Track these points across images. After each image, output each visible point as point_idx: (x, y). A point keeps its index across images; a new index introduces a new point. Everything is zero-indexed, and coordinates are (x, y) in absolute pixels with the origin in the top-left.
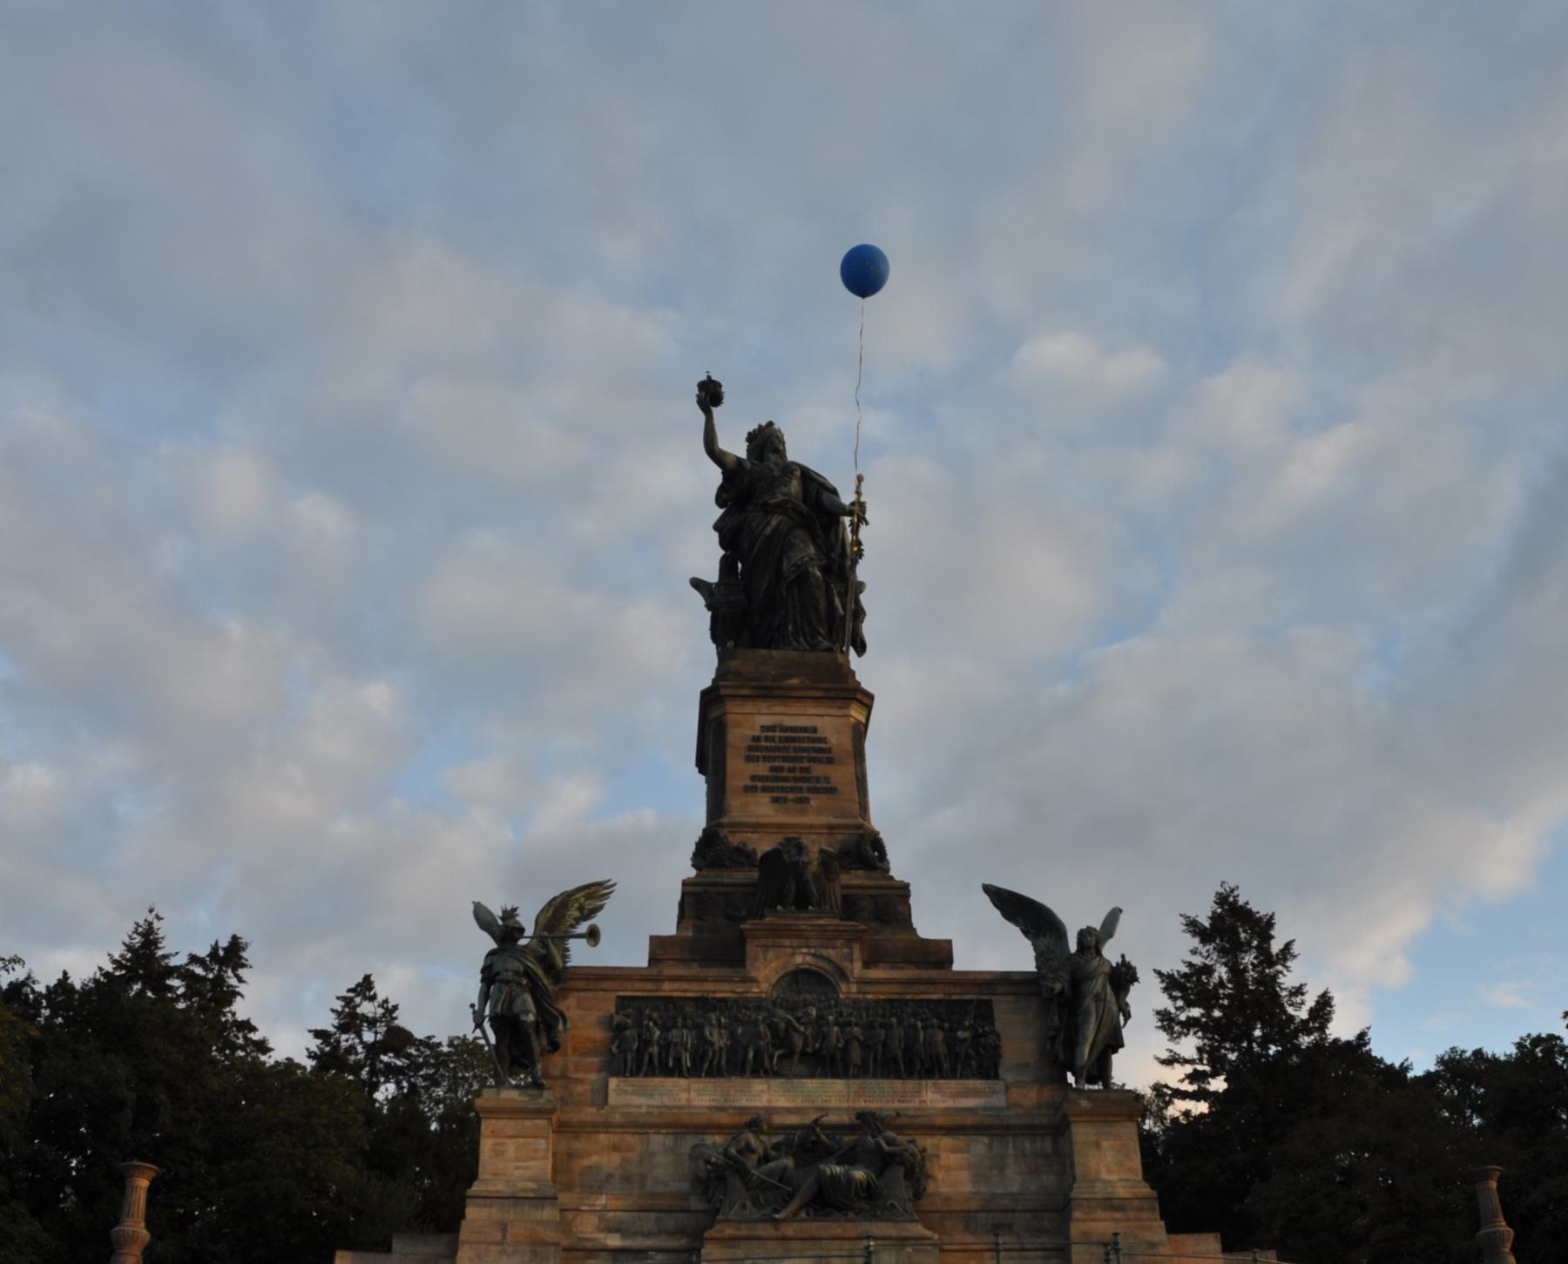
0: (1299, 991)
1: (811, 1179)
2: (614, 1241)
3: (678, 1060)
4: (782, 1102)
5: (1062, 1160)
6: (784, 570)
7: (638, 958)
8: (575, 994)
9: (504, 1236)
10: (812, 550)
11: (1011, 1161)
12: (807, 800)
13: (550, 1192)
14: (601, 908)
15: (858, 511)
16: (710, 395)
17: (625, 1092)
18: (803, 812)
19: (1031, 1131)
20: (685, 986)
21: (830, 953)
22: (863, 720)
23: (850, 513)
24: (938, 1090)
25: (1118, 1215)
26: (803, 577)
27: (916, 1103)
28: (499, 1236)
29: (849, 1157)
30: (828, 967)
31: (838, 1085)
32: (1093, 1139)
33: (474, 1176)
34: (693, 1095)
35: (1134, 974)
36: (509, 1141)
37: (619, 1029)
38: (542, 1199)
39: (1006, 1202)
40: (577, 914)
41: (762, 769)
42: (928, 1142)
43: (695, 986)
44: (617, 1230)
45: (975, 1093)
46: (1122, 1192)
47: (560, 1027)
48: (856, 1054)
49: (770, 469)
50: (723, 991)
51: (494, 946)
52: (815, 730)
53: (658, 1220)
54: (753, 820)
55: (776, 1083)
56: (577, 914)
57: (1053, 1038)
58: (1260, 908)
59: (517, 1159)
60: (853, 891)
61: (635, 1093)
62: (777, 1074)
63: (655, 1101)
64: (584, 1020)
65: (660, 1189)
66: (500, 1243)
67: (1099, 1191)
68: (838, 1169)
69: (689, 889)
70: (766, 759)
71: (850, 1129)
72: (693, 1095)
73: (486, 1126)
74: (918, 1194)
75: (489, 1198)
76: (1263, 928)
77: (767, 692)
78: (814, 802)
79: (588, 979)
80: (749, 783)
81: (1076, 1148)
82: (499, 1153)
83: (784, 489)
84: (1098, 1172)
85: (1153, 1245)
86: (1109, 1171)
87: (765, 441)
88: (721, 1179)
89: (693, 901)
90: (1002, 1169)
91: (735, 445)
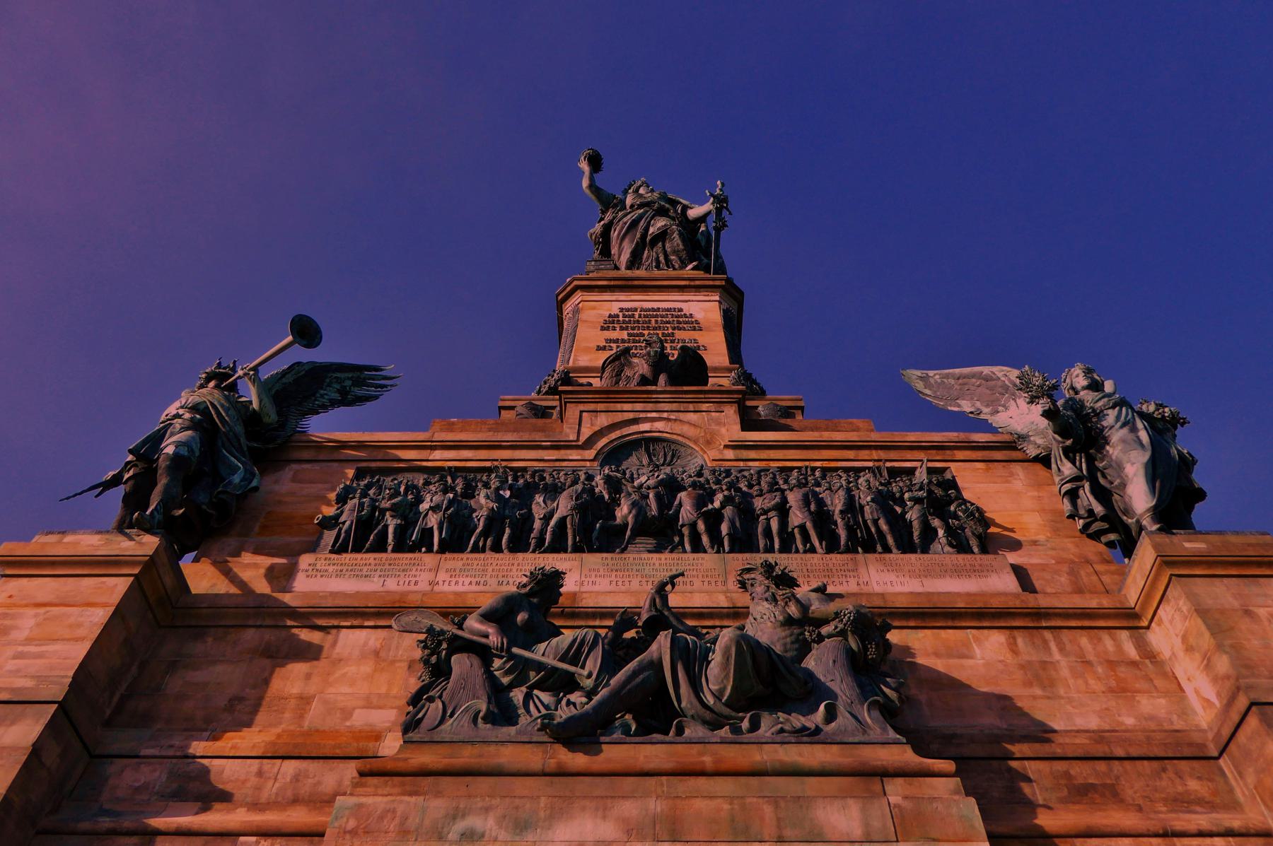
3: (428, 533)
8: (294, 466)
11: (1065, 672)
14: (377, 397)
21: (692, 417)
22: (735, 312)
40: (337, 396)
52: (681, 310)
56: (337, 396)
57: (1073, 495)
61: (339, 574)
70: (622, 329)
72: (442, 576)
80: (603, 344)
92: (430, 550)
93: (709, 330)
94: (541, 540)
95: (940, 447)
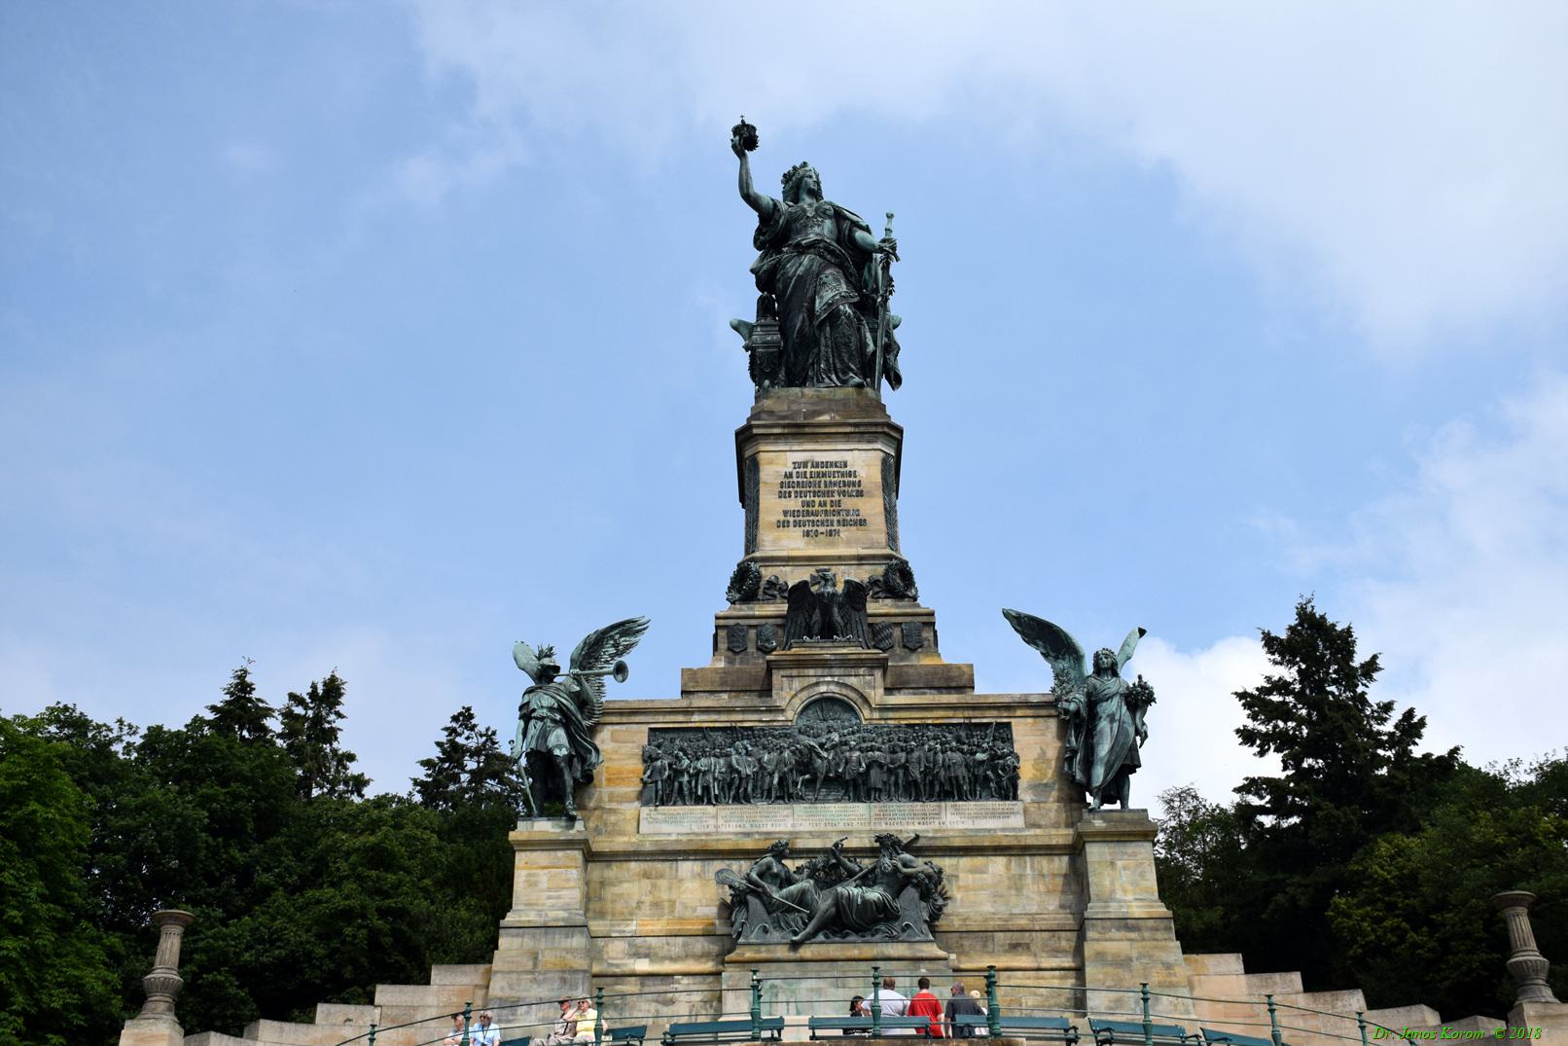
0: (1388, 707)
1: (829, 901)
2: (643, 966)
3: (706, 789)
4: (805, 826)
5: (1077, 880)
6: (820, 310)
7: (669, 692)
9: (535, 965)
10: (844, 288)
11: (1029, 881)
12: (838, 532)
13: (580, 920)
15: (889, 250)
16: (745, 139)
17: (656, 821)
18: (833, 545)
19: (1048, 851)
20: (714, 717)
21: (853, 681)
23: (881, 250)
24: (957, 811)
25: (1133, 935)
26: (834, 316)
27: (936, 826)
28: (530, 965)
29: (868, 880)
30: (852, 695)
31: (861, 808)
32: (1109, 858)
33: (509, 907)
34: (721, 821)
35: (1151, 694)
36: (541, 872)
37: (648, 759)
38: (570, 927)
39: (1023, 922)
40: (612, 651)
41: (794, 504)
42: (946, 863)
43: (724, 717)
44: (647, 956)
45: (994, 815)
46: (1137, 911)
47: (593, 759)
48: (876, 777)
49: (804, 211)
50: (751, 720)
51: (532, 684)
53: (685, 945)
54: (784, 553)
55: (800, 808)
56: (612, 651)
57: (1070, 760)
58: (1339, 620)
59: (549, 889)
60: (879, 620)
62: (801, 799)
63: (685, 829)
64: (619, 752)
65: (688, 914)
66: (531, 972)
67: (1114, 910)
68: (856, 891)
69: (722, 622)
70: (798, 494)
71: (871, 852)
72: (721, 821)
73: (520, 859)
74: (936, 914)
75: (520, 928)
76: (1343, 643)
77: (798, 431)
78: (845, 533)
79: (621, 714)
81: (1090, 869)
82: (532, 884)
83: (817, 229)
84: (1113, 891)
85: (1168, 966)
86: (1125, 891)
87: (798, 184)
88: (744, 903)
89: (730, 636)
90: (1019, 889)
91: (771, 190)
92: (709, 803)
93: (872, 496)
94: (769, 791)
95: (1009, 707)
